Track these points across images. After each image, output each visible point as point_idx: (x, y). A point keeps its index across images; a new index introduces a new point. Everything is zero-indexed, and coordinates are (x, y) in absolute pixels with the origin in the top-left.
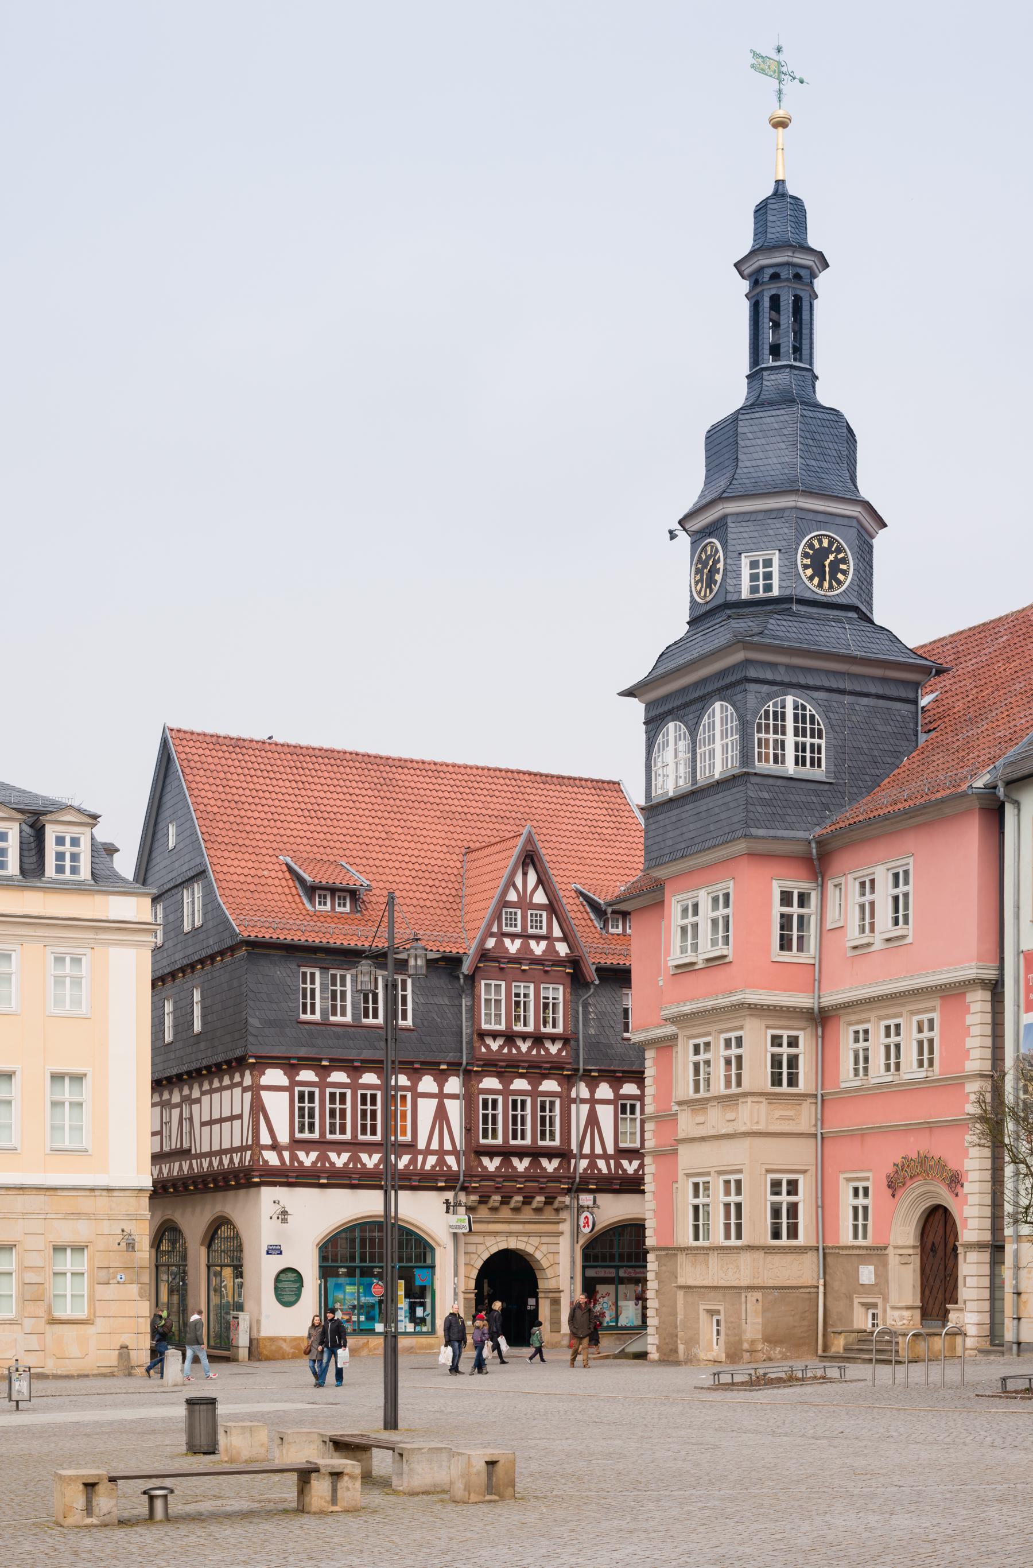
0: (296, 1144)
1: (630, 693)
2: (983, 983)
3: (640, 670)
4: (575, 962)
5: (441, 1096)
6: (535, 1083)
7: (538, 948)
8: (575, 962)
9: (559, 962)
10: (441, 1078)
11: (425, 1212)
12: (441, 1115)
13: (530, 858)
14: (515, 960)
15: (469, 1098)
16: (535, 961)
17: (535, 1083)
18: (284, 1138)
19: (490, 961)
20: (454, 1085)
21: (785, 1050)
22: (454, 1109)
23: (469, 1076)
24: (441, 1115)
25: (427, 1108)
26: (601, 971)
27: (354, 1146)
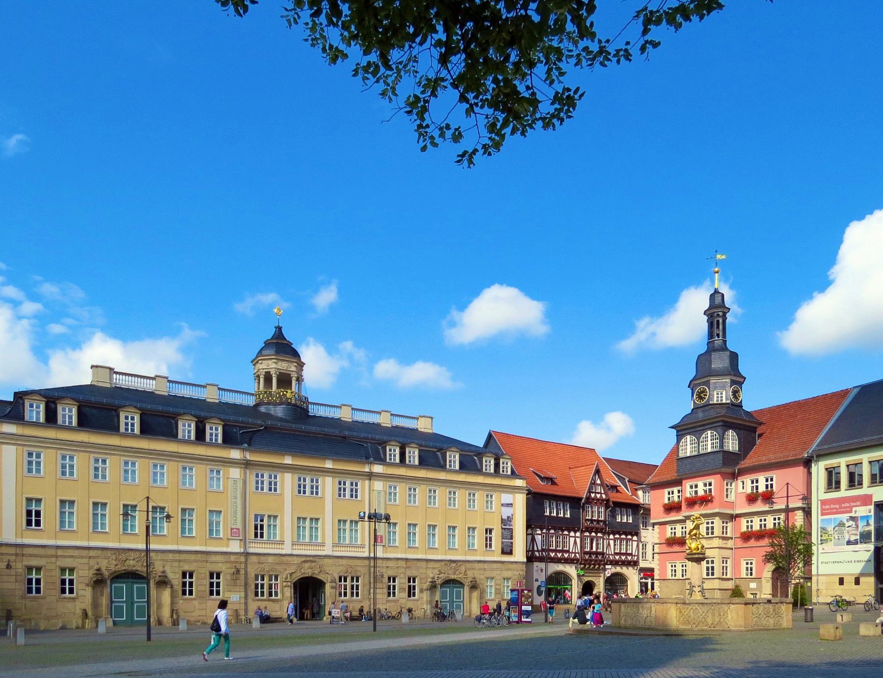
0: (543, 550)
1: (672, 427)
2: (803, 509)
3: (677, 420)
4: (608, 500)
5: (575, 537)
6: (590, 533)
7: (598, 496)
8: (608, 500)
9: (603, 500)
10: (575, 532)
11: (571, 570)
12: (575, 542)
13: (598, 472)
14: (593, 499)
15: (582, 539)
16: (598, 500)
17: (590, 533)
18: (540, 548)
19: (589, 500)
20: (578, 534)
21: (710, 525)
22: (578, 540)
23: (582, 532)
24: (575, 542)
25: (572, 540)
26: (614, 503)
27: (556, 551)
